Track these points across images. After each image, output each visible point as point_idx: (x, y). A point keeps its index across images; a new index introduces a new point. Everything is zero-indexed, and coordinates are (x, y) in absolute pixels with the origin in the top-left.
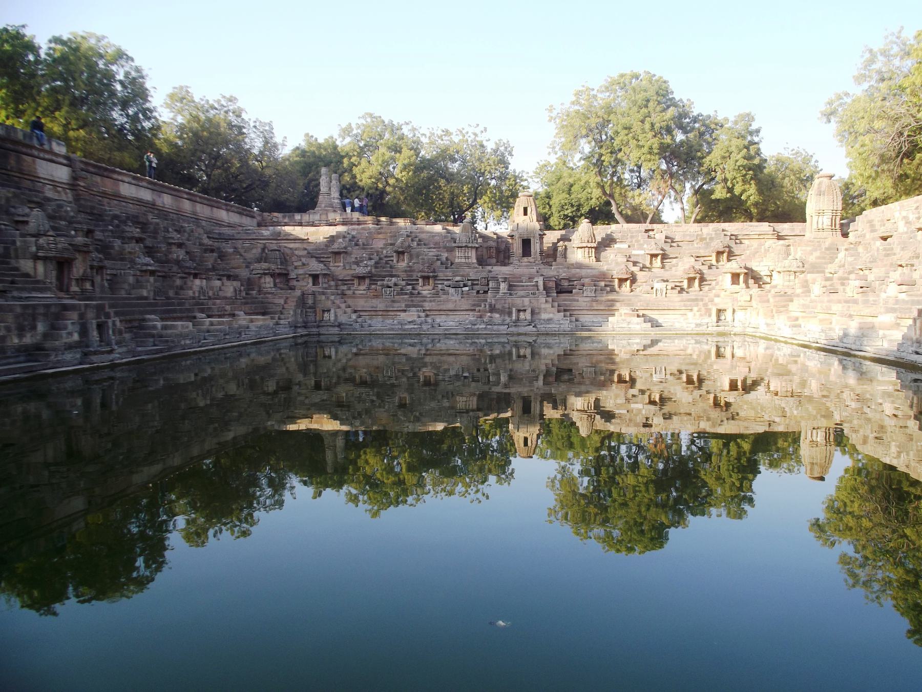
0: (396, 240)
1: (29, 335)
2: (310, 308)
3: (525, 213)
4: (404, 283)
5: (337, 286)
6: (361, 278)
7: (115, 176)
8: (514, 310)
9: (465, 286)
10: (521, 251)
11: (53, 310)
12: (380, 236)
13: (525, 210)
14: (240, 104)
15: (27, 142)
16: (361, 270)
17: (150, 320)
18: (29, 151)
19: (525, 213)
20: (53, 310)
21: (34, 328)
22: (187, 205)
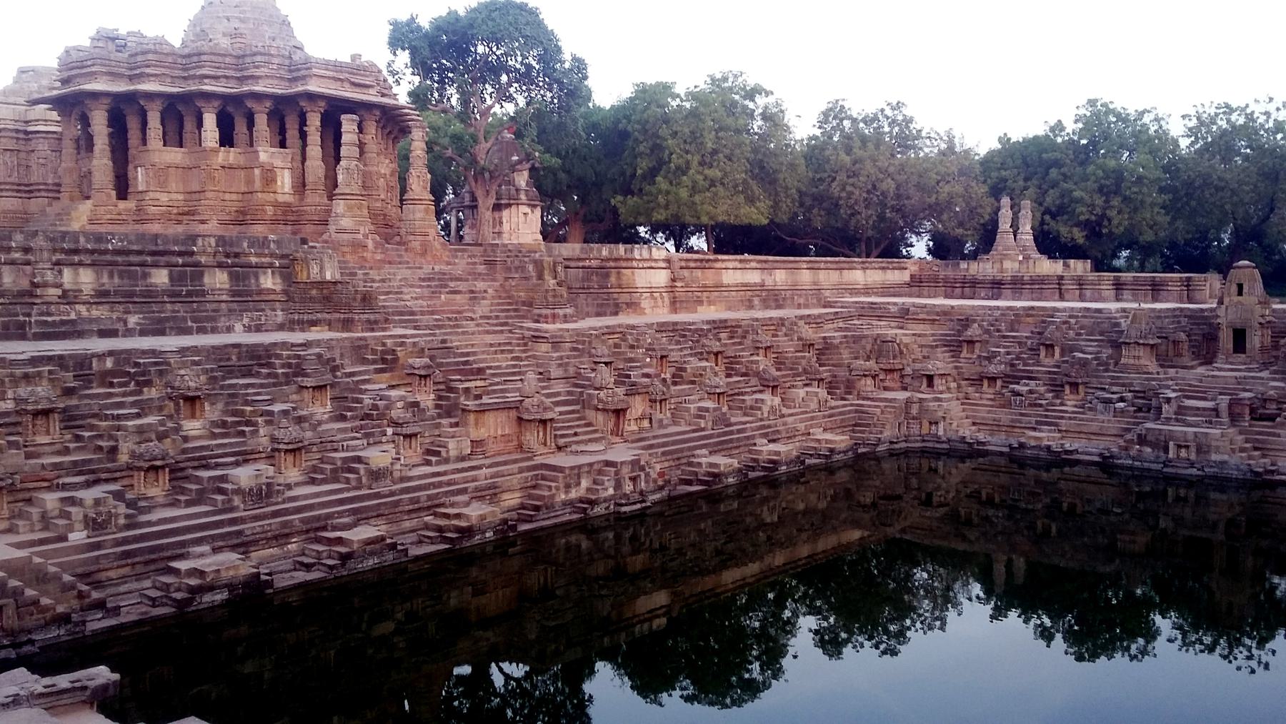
0: (1046, 328)
1: (574, 491)
2: (913, 418)
3: (1240, 293)
4: (1042, 389)
5: (959, 386)
6: (992, 380)
7: (718, 265)
8: (1171, 444)
9: (1122, 400)
10: (1231, 346)
11: (596, 467)
12: (1030, 320)
13: (1240, 287)
14: (908, 112)
15: (629, 256)
16: (993, 369)
17: (699, 456)
18: (629, 264)
19: (1240, 293)
20: (596, 467)
21: (579, 484)
22: (805, 277)
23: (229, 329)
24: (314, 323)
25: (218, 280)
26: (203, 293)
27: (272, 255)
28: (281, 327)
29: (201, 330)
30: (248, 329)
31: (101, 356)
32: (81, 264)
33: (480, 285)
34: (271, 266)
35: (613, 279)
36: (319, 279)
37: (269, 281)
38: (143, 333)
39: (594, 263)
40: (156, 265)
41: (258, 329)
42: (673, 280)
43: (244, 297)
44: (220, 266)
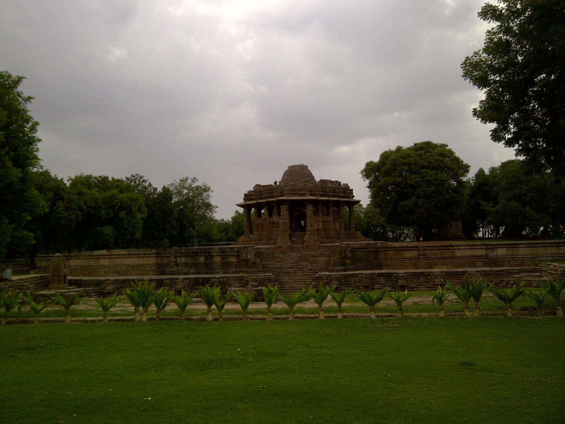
23: (218, 273)
24: (241, 272)
25: (217, 259)
26: (214, 263)
27: (235, 252)
28: (234, 273)
29: (210, 273)
30: (223, 273)
31: (166, 279)
32: (182, 256)
33: (320, 259)
34: (234, 255)
35: (382, 256)
36: (246, 258)
37: (233, 259)
38: (194, 274)
39: (372, 250)
40: (201, 256)
41: (227, 273)
42: (419, 255)
43: (225, 265)
44: (219, 255)
